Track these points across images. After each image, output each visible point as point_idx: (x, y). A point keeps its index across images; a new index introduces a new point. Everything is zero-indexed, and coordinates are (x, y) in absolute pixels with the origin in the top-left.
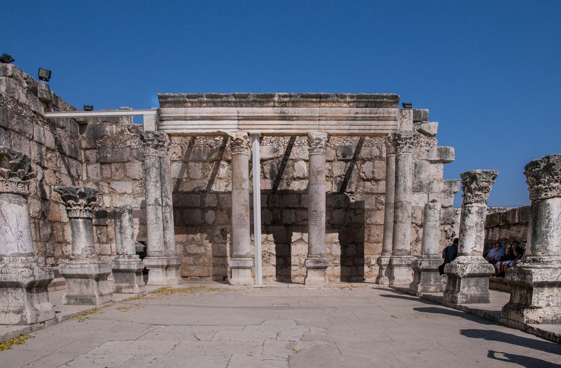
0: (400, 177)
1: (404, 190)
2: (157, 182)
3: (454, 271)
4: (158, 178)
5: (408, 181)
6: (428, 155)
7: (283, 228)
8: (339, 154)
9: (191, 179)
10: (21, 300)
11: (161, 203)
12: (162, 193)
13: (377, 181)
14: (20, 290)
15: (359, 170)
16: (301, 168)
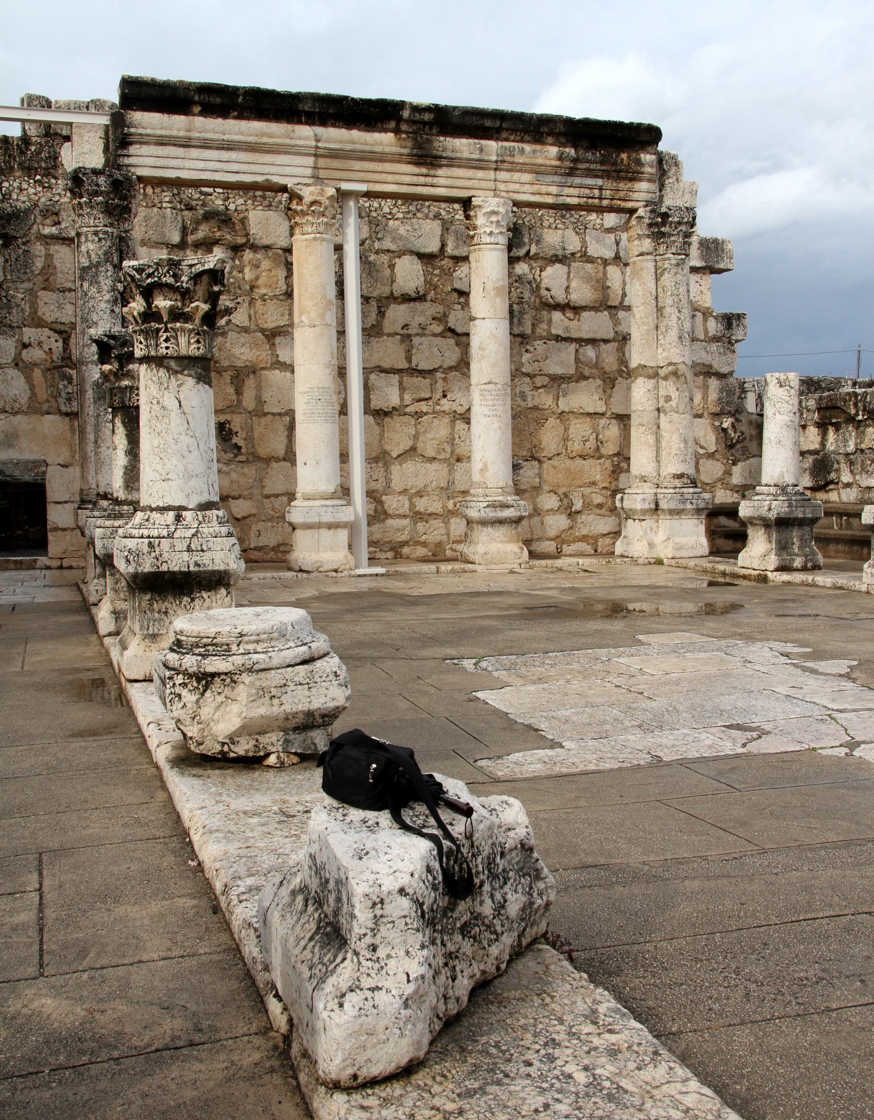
1: (680, 338)
14: (223, 591)
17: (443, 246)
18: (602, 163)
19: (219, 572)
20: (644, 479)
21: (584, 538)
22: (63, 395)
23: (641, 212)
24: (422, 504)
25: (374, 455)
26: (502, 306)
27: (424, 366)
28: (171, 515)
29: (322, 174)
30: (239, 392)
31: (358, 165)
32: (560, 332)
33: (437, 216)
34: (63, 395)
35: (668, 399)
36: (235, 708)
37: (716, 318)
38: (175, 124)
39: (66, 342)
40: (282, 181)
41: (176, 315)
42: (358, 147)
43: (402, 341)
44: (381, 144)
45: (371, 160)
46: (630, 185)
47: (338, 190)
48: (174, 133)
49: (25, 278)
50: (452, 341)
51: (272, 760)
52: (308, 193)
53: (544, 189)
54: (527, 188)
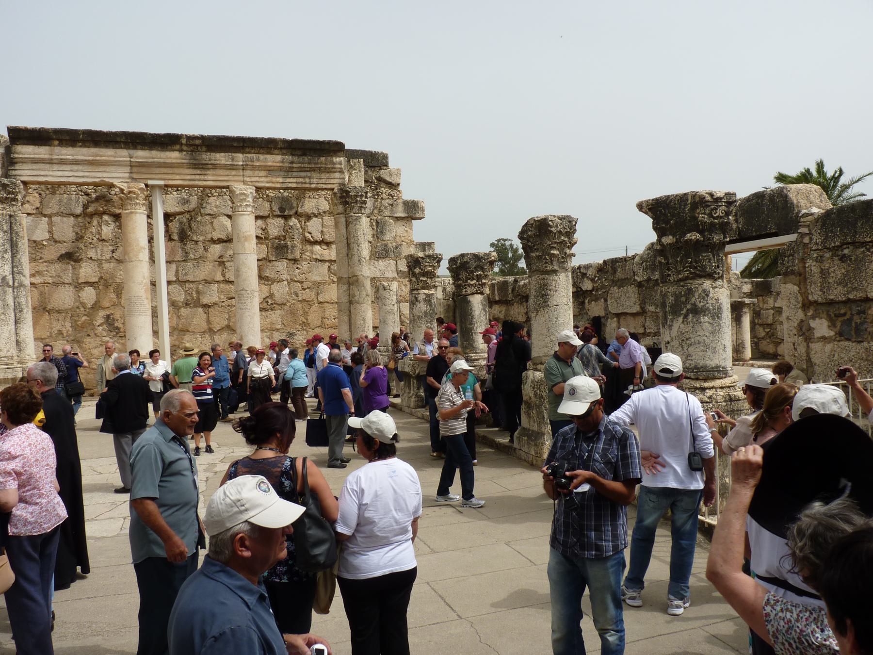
0: (352, 245)
2: (5, 251)
4: (8, 246)
5: (365, 251)
6: (391, 210)
7: (201, 310)
8: (276, 208)
9: (56, 242)
11: (11, 283)
12: (13, 267)
13: (328, 244)
15: (304, 230)
16: (224, 227)
18: (309, 163)
23: (336, 190)
25: (203, 330)
29: (135, 176)
30: (119, 296)
31: (158, 170)
35: (354, 296)
38: (42, 152)
40: (111, 181)
42: (156, 160)
43: (219, 265)
44: (170, 158)
45: (165, 167)
46: (328, 175)
47: (147, 185)
48: (42, 156)
52: (125, 187)
53: (274, 180)
54: (262, 180)
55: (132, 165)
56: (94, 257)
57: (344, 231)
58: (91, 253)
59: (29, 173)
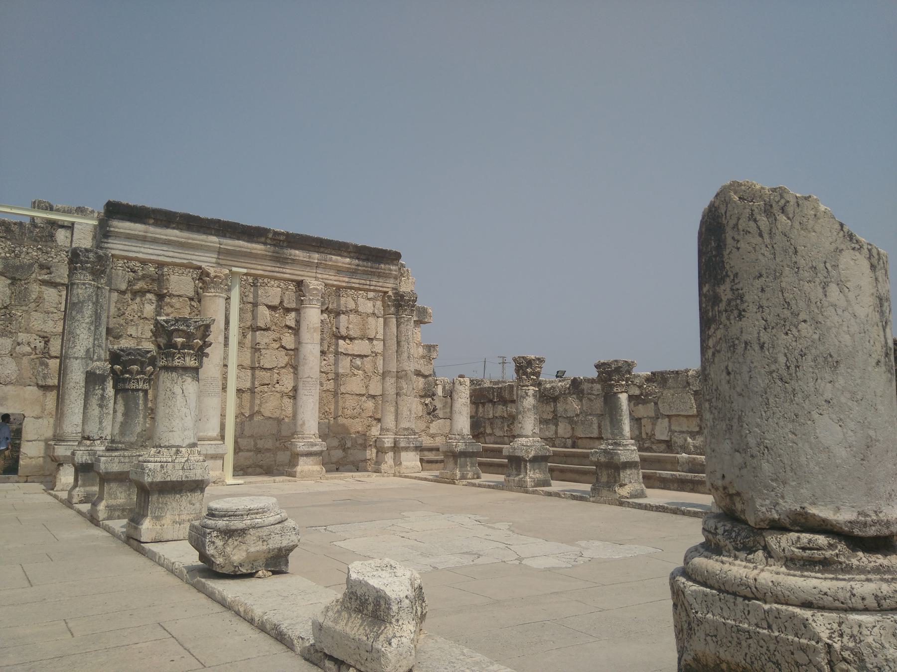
3: (518, 453)
10: (198, 505)
12: (94, 340)
13: (351, 339)
17: (281, 302)
18: (371, 267)
19: (198, 481)
20: (388, 430)
21: (353, 463)
22: (41, 374)
23: (390, 293)
24: (261, 444)
26: (317, 337)
27: (267, 366)
28: (174, 449)
29: (221, 262)
32: (342, 350)
33: (278, 287)
34: (41, 374)
35: (401, 388)
36: (244, 547)
37: (423, 346)
39: (46, 343)
41: (184, 346)
49: (24, 303)
50: (284, 352)
51: (260, 573)
53: (341, 279)
54: (331, 277)
55: (220, 252)
56: (134, 335)
57: (395, 330)
58: (131, 330)
59: (121, 247)
